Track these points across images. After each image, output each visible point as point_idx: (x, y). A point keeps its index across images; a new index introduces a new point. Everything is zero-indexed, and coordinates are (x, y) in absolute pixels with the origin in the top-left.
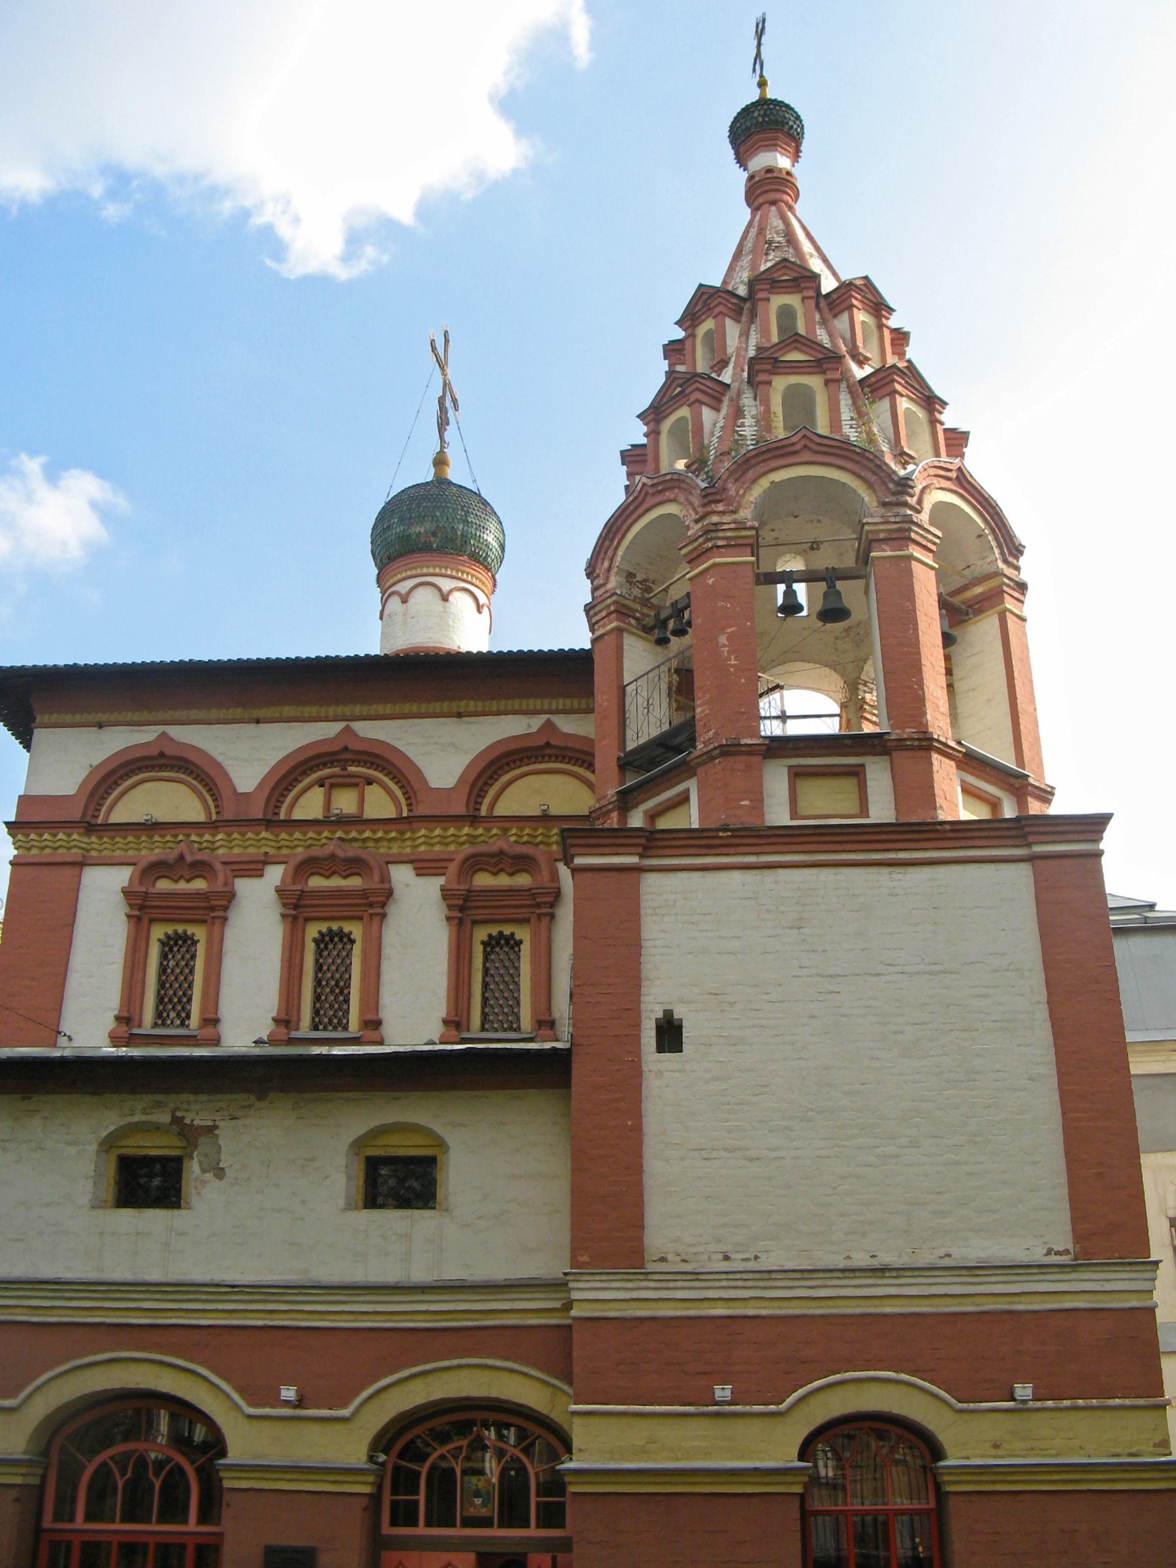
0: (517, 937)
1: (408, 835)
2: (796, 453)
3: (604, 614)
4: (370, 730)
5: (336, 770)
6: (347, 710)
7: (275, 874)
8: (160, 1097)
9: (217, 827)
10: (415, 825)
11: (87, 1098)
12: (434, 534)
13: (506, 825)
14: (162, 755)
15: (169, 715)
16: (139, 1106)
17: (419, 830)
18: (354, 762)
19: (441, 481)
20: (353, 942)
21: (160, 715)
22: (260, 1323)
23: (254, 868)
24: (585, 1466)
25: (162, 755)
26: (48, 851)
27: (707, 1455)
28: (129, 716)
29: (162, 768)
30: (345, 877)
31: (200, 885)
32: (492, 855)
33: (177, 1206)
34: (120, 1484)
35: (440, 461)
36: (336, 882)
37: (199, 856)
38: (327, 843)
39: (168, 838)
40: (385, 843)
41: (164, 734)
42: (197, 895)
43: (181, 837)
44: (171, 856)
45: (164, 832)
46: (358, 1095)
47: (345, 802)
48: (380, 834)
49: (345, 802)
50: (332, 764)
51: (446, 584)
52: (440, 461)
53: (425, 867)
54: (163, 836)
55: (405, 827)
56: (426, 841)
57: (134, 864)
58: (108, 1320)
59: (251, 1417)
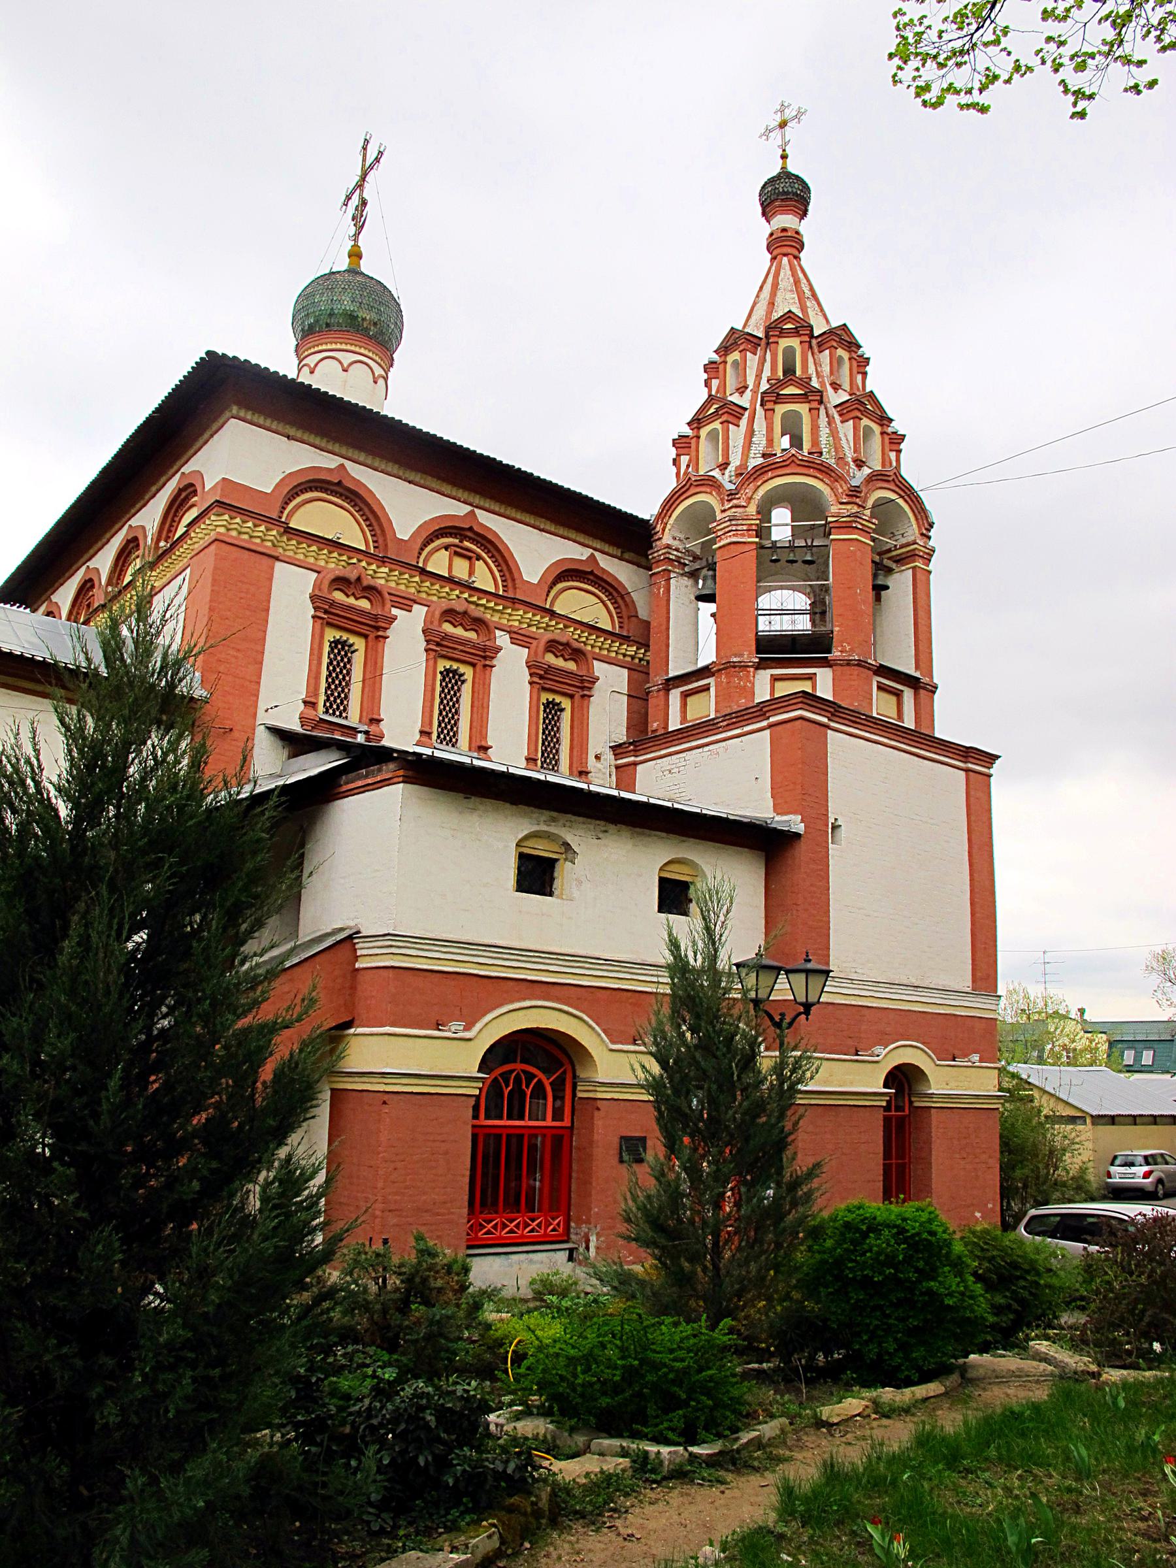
0: (563, 706)
1: (509, 611)
2: (888, 481)
3: (745, 528)
4: (485, 519)
5: (456, 541)
6: (477, 500)
7: (420, 611)
8: (555, 814)
9: (384, 562)
10: (517, 606)
11: (508, 805)
12: (375, 324)
13: (568, 623)
14: (339, 483)
15: (350, 453)
16: (543, 818)
17: (518, 610)
18: (472, 541)
19: (354, 271)
20: (463, 682)
21: (343, 451)
22: (616, 986)
23: (406, 603)
24: (815, 1089)
25: (339, 483)
26: (246, 537)
27: (852, 1084)
28: (317, 441)
29: (333, 493)
30: (466, 630)
31: (364, 604)
32: (561, 644)
33: (551, 894)
34: (506, 1093)
35: (355, 254)
36: (459, 631)
37: (372, 582)
38: (457, 599)
39: (345, 558)
40: (482, 609)
41: (342, 465)
42: (362, 612)
43: (354, 561)
44: (353, 576)
45: (342, 552)
46: (664, 834)
47: (461, 569)
48: (492, 604)
49: (461, 569)
50: (455, 536)
51: (347, 358)
52: (355, 254)
53: (519, 638)
54: (340, 555)
55: (509, 604)
56: (518, 618)
57: (318, 572)
58: (529, 978)
59: (612, 1050)
